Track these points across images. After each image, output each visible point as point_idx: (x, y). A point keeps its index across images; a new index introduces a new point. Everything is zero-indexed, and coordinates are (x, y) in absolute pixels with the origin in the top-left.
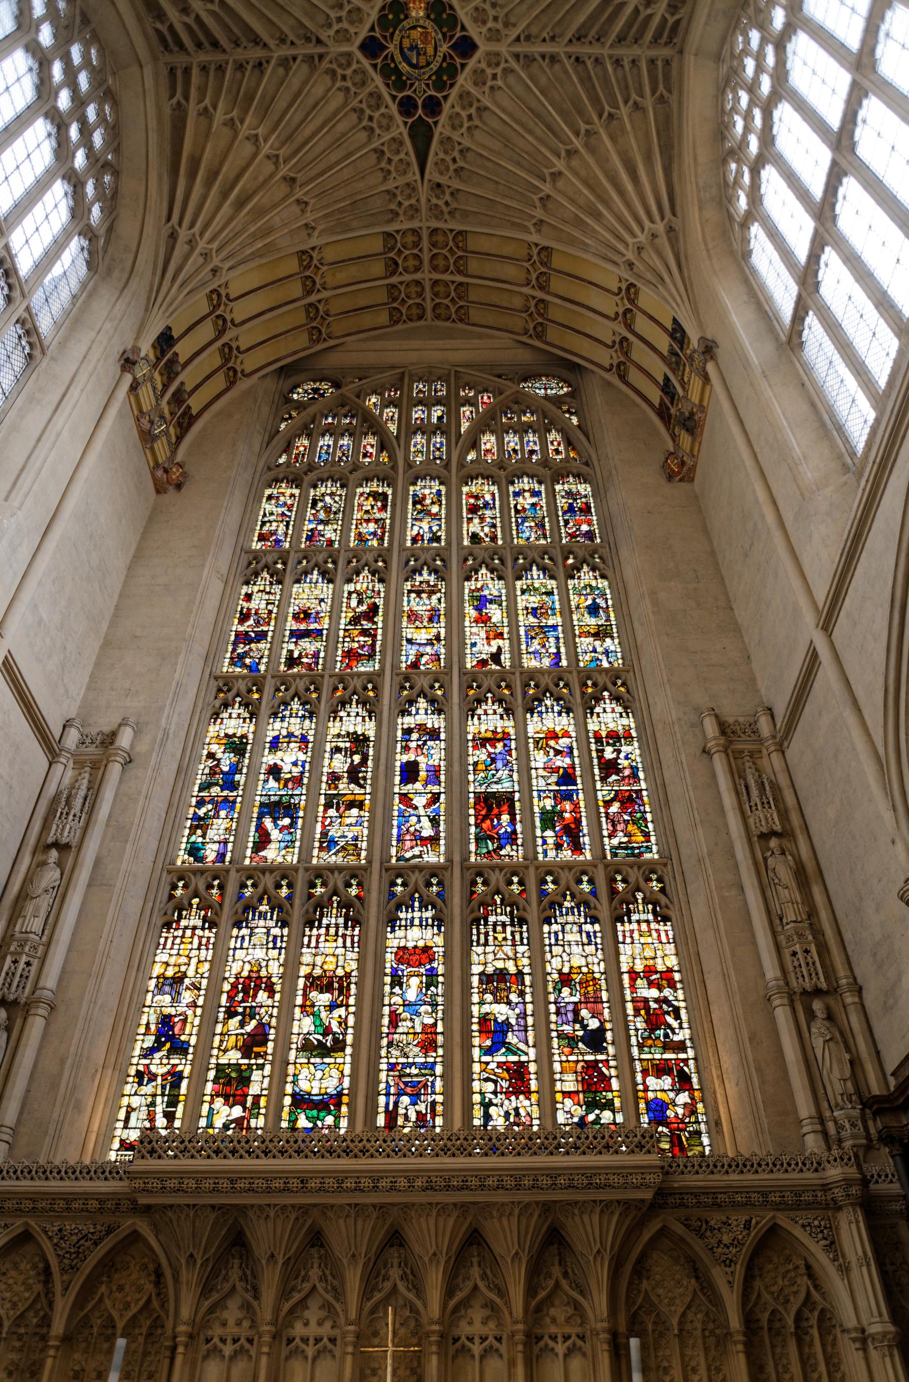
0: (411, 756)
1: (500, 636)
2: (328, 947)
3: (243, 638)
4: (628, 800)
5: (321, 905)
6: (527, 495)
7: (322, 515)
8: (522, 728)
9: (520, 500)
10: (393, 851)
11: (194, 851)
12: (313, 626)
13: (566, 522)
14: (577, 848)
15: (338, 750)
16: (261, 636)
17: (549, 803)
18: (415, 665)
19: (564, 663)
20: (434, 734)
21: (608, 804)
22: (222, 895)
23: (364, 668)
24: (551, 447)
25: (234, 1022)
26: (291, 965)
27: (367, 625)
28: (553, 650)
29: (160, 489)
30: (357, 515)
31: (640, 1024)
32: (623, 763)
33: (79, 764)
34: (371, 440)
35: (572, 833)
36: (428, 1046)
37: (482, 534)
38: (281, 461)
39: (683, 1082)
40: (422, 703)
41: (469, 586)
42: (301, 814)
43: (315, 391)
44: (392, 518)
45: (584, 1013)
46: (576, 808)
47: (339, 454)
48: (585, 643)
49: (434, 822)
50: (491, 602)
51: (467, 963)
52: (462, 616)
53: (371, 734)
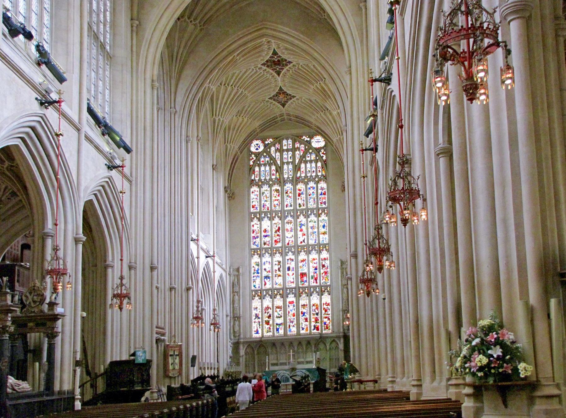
0: (289, 265)
1: (304, 235)
3: (254, 238)
4: (326, 273)
5: (276, 295)
6: (312, 189)
8: (308, 257)
9: (310, 190)
10: (287, 285)
11: (254, 286)
12: (268, 234)
13: (320, 198)
14: (317, 283)
15: (276, 264)
16: (258, 237)
17: (312, 274)
18: (288, 244)
20: (292, 260)
21: (322, 274)
22: (261, 294)
23: (279, 245)
24: (318, 170)
25: (266, 314)
26: (273, 305)
27: (278, 233)
28: (315, 238)
29: (229, 200)
30: (273, 198)
31: (323, 311)
32: (326, 265)
34: (273, 168)
35: (316, 279)
36: (294, 316)
37: (301, 204)
38: (253, 178)
40: (290, 253)
41: (299, 220)
42: (271, 278)
43: (257, 144)
44: (281, 199)
45: (316, 310)
46: (317, 275)
47: (266, 174)
48: (321, 236)
49: (293, 278)
50: (303, 225)
51: (299, 303)
52: (297, 229)
53: (281, 260)
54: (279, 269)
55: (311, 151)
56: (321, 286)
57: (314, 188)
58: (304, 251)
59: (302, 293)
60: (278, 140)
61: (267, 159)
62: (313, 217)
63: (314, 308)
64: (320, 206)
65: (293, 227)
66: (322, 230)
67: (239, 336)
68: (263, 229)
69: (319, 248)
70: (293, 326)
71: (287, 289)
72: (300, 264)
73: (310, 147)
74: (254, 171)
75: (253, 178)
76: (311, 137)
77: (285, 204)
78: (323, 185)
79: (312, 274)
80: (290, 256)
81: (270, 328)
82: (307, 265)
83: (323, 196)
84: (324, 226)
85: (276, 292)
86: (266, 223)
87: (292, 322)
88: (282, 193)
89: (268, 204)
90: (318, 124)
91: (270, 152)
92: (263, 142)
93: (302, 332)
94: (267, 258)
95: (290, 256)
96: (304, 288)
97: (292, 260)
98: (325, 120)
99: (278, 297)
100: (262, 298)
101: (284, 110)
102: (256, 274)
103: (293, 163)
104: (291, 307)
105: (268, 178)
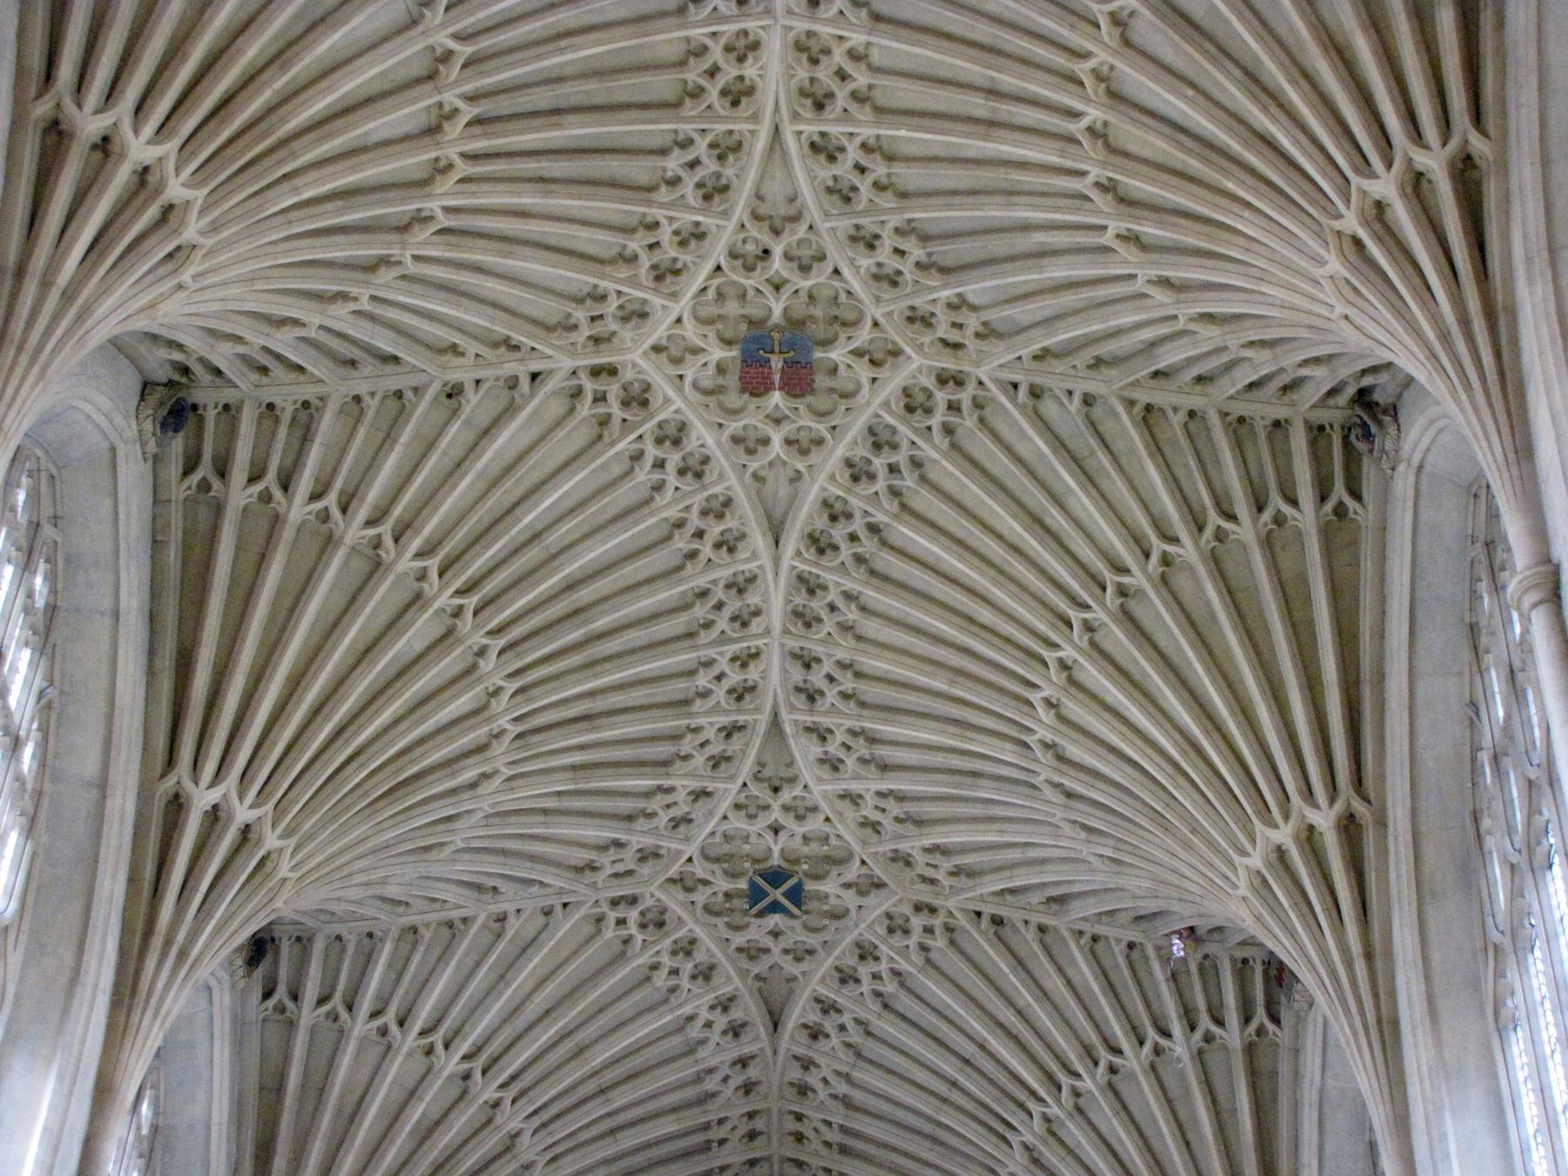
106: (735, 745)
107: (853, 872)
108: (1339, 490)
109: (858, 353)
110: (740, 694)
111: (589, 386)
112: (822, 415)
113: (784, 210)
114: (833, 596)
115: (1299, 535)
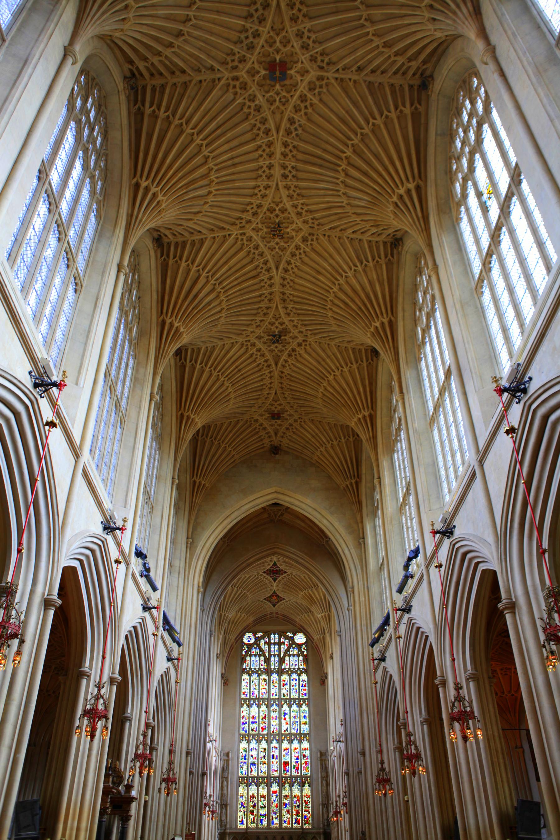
1: (287, 724)
2: (262, 791)
3: (243, 723)
4: (306, 763)
5: (261, 783)
7: (254, 687)
11: (241, 772)
12: (255, 720)
14: (298, 773)
16: (246, 723)
18: (273, 732)
19: (299, 731)
20: (276, 748)
23: (265, 732)
27: (264, 720)
30: (261, 687)
31: (304, 804)
32: (306, 755)
33: (224, 760)
34: (262, 658)
35: (297, 769)
36: (277, 807)
38: (244, 667)
39: (309, 813)
41: (283, 709)
48: (302, 726)
51: (282, 793)
54: (264, 758)
55: (294, 646)
56: (301, 777)
57: (296, 680)
58: (287, 740)
59: (285, 783)
60: (267, 634)
61: (257, 651)
62: (295, 707)
63: (295, 799)
64: (301, 697)
65: (278, 715)
66: (303, 720)
67: (226, 825)
68: (251, 716)
69: (300, 737)
70: (276, 818)
71: (271, 777)
72: (284, 753)
73: (294, 643)
74: (246, 660)
75: (244, 667)
76: (295, 634)
77: (271, 693)
78: (304, 677)
79: (294, 764)
80: (275, 744)
81: (254, 819)
82: (289, 754)
83: (304, 688)
84: (305, 717)
85: (261, 780)
86: (254, 710)
87: (275, 814)
88: (269, 682)
89: (256, 692)
90: (301, 623)
91: (260, 644)
92: (254, 635)
93: (284, 825)
94: (254, 744)
95: (275, 744)
96: (286, 778)
97: (276, 748)
98: (309, 622)
99: (263, 785)
100: (248, 785)
101: (274, 609)
102: (243, 760)
103: (279, 655)
104: (274, 797)
105: (257, 668)
106: (269, 396)
107: (288, 413)
108: (370, 360)
109: (290, 337)
110: (270, 388)
111: (245, 343)
112: (283, 346)
113: (278, 316)
114: (286, 374)
115: (363, 367)
